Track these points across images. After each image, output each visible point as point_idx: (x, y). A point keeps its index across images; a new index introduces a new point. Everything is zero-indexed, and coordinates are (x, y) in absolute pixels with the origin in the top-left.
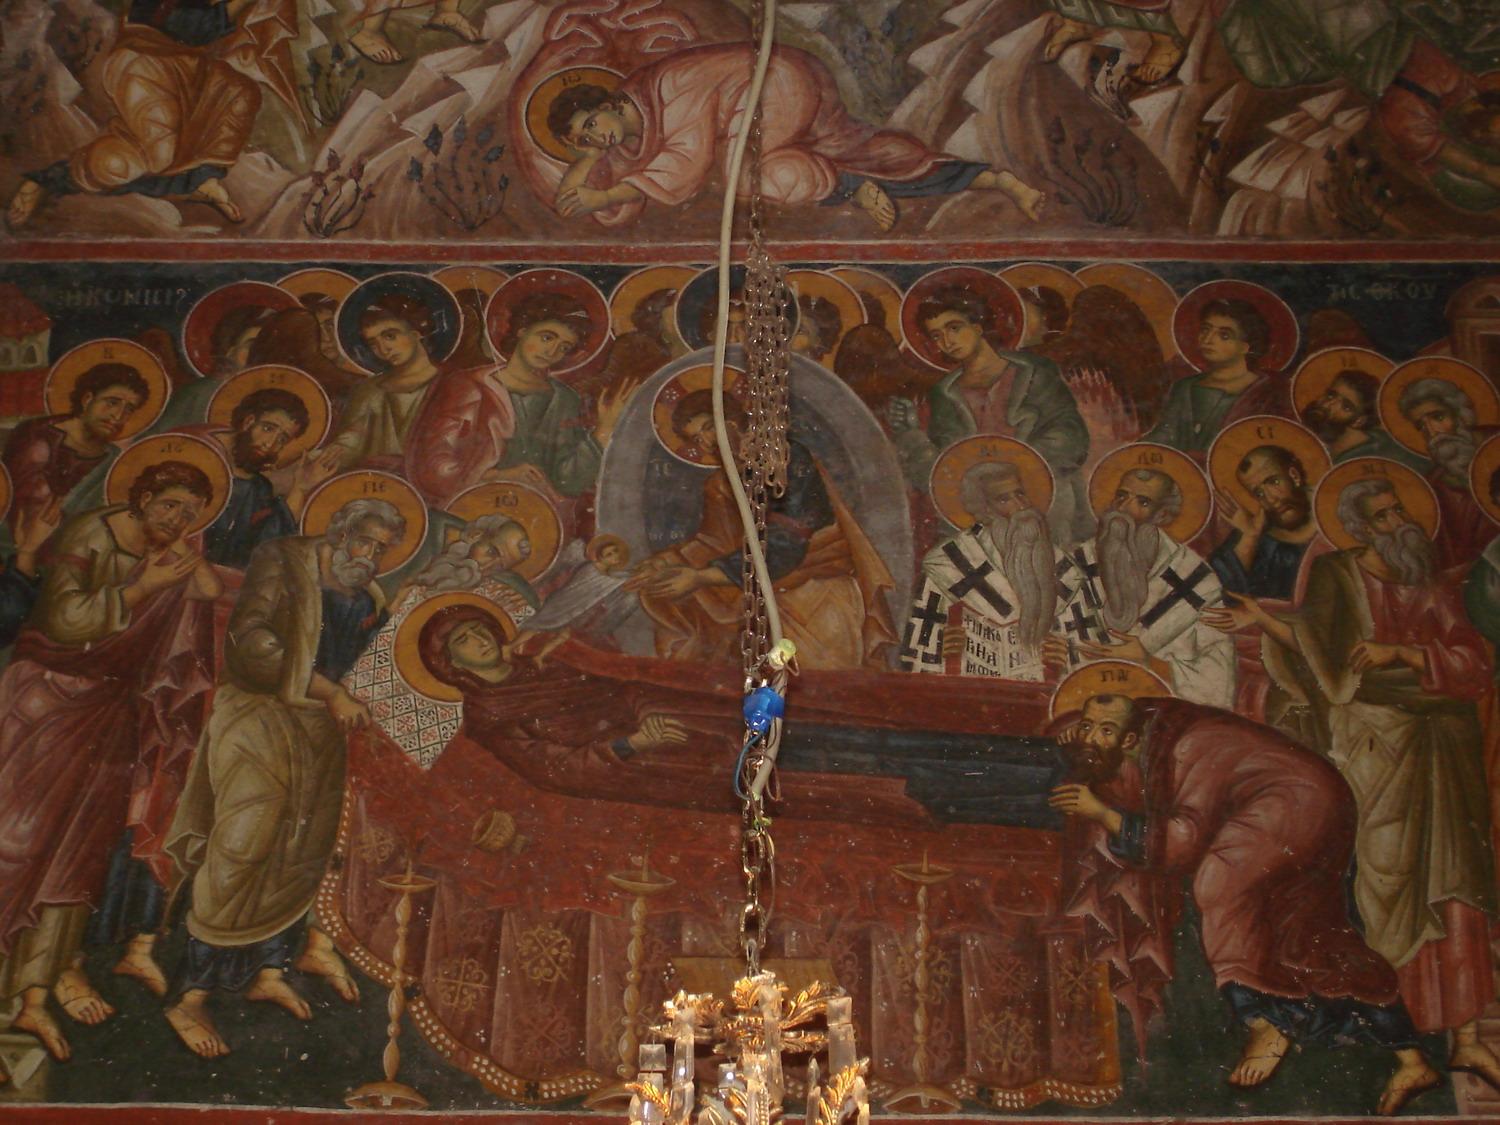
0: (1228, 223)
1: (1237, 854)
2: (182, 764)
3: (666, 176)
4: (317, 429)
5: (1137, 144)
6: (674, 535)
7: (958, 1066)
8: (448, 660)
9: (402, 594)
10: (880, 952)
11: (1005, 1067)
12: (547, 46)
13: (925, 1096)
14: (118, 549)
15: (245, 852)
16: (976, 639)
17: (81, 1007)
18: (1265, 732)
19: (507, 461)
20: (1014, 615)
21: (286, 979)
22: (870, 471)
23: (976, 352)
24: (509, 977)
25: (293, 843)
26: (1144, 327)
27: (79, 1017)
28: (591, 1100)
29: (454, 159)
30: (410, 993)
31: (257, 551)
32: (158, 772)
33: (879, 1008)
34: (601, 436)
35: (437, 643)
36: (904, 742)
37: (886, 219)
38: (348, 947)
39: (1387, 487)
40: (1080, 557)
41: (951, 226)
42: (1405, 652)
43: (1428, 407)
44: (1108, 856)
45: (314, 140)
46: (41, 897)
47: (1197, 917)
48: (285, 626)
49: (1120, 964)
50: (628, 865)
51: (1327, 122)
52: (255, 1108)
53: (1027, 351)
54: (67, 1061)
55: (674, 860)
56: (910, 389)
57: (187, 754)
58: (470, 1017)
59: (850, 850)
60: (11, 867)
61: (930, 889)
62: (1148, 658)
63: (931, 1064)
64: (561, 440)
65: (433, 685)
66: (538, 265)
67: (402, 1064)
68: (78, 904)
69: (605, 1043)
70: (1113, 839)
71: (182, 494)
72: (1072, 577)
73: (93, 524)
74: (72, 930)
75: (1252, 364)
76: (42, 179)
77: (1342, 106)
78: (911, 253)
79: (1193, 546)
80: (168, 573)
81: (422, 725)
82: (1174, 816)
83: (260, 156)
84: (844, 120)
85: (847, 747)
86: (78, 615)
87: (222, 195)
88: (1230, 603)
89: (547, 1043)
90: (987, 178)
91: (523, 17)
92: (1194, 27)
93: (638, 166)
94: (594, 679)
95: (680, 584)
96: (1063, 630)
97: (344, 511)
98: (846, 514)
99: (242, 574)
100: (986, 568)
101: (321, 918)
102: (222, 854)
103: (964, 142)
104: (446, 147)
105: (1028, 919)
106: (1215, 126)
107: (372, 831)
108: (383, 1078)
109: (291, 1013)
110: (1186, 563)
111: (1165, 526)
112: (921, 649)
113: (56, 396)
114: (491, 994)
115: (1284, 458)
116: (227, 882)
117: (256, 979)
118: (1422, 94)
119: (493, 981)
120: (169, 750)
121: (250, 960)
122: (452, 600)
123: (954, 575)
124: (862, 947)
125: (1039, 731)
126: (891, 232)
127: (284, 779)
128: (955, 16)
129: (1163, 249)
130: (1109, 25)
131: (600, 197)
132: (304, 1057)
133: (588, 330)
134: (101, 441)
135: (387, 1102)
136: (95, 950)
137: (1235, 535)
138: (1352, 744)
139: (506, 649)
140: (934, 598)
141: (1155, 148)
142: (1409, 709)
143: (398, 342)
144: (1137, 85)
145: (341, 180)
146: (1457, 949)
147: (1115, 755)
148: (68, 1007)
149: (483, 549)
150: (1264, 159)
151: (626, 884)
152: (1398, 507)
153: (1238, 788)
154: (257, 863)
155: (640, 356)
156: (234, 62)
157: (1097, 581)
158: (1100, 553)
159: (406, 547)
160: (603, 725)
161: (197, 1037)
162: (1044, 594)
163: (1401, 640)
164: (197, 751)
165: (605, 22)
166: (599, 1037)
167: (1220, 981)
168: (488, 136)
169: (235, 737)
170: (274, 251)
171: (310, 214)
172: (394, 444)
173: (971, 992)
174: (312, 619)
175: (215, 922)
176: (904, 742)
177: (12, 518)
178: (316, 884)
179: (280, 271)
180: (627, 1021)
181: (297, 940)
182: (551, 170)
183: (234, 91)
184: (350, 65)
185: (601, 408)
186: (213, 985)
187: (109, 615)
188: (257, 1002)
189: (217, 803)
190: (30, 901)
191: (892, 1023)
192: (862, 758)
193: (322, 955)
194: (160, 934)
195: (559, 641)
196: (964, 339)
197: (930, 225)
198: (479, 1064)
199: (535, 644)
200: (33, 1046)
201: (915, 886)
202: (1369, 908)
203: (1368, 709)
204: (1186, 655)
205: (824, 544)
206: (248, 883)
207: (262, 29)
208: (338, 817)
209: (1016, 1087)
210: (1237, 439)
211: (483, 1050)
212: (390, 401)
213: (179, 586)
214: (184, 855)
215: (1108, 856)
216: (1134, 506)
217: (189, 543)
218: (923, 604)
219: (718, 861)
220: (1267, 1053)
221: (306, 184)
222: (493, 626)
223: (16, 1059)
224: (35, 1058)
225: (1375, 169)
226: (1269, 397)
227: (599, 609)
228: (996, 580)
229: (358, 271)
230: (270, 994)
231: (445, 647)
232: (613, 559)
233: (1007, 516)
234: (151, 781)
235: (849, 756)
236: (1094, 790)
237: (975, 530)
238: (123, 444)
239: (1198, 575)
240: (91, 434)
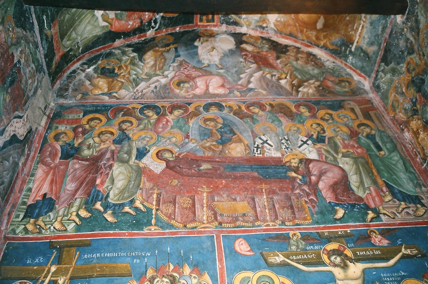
0: (300, 95)
1: (326, 181)
2: (108, 174)
3: (198, 91)
4: (134, 125)
5: (281, 86)
6: (205, 138)
7: (277, 218)
8: (162, 157)
9: (152, 147)
10: (257, 200)
11: (287, 218)
12: (175, 76)
13: (271, 224)
14: (95, 143)
16: (267, 151)
18: (326, 162)
19: (172, 127)
20: (273, 147)
21: (130, 208)
22: (242, 128)
23: (259, 112)
24: (178, 207)
25: (131, 186)
26: (289, 108)
28: (198, 228)
29: (159, 90)
30: (157, 210)
31: (123, 142)
33: (258, 209)
34: (190, 124)
35: (159, 154)
36: (256, 167)
37: (239, 95)
38: (143, 202)
39: (338, 127)
40: (284, 138)
41: (251, 96)
42: (349, 150)
43: (342, 117)
44: (300, 183)
45: (133, 88)
47: (321, 191)
48: (129, 153)
49: (307, 200)
50: (202, 187)
51: (314, 83)
52: (123, 232)
53: (268, 111)
54: (80, 225)
55: (212, 186)
56: (248, 117)
57: (109, 173)
58: (170, 214)
59: (248, 183)
61: (265, 190)
62: (301, 152)
63: (271, 218)
64: (182, 125)
65: (159, 161)
66: (176, 102)
67: (156, 223)
69: (200, 217)
70: (300, 180)
71: (109, 135)
72: (283, 141)
73: (91, 139)
75: (309, 112)
76: (83, 94)
77: (316, 81)
78: (244, 99)
79: (305, 136)
80: (106, 146)
81: (158, 167)
82: (312, 176)
83: (124, 90)
84: (229, 83)
85: (245, 168)
86: (86, 153)
87: (116, 95)
88: (314, 144)
89: (188, 218)
90: (256, 90)
91: (171, 72)
92: (288, 72)
93: (193, 90)
94: (192, 159)
95: (208, 144)
96: (284, 149)
97: (140, 136)
98: (238, 134)
99: (120, 146)
100: (267, 140)
103: (251, 86)
104: (158, 89)
105: (286, 194)
106: (294, 84)
107: (148, 184)
108: (152, 225)
109: (132, 214)
110: (305, 139)
111: (300, 134)
112: (257, 153)
113: (84, 121)
114: (175, 210)
115: (319, 125)
117: (123, 208)
118: (329, 80)
119: (175, 207)
120: (104, 173)
121: (122, 205)
122: (163, 148)
123: (262, 142)
124: (253, 199)
125: (282, 164)
126: (241, 97)
128: (246, 71)
129: (290, 98)
130: (273, 72)
131: (186, 94)
132: (134, 222)
133: (186, 110)
134: (92, 128)
135: (153, 229)
136: (88, 204)
137: (312, 135)
138: (343, 164)
139: (174, 155)
140: (258, 145)
141: (285, 86)
142: (353, 158)
143: (150, 113)
144: (280, 79)
145: (139, 93)
146: (374, 194)
147: (298, 167)
149: (168, 141)
150: (304, 88)
151: (202, 190)
152: (341, 130)
153: (323, 171)
154: (123, 189)
155: (196, 114)
156: (119, 79)
157: (288, 142)
158: (288, 137)
159: (153, 141)
160: (194, 166)
161: (110, 219)
162: (279, 144)
163: (347, 148)
164: (111, 172)
165: (185, 73)
166: (199, 216)
167: (328, 201)
168: (165, 87)
169: (119, 170)
170: (127, 102)
171: (133, 97)
172: (150, 127)
173: (277, 206)
174: (134, 152)
176: (256, 167)
177: (74, 139)
178: (136, 192)
179: (127, 104)
180: (204, 213)
181: (132, 202)
182: (177, 91)
183: (119, 83)
184: (140, 79)
185: (189, 120)
186: (114, 209)
187: (93, 152)
191: (262, 211)
192: (248, 169)
193: (138, 204)
195: (184, 154)
196: (257, 110)
197: (247, 96)
198: (173, 222)
199: (179, 154)
201: (262, 189)
202: (355, 189)
203: (345, 159)
204: (308, 152)
205: (235, 138)
207: (124, 76)
208: (141, 181)
209: (290, 221)
210: (311, 121)
211: (174, 219)
212: (149, 121)
213: (107, 148)
215: (300, 183)
216: (293, 131)
217: (109, 142)
218: (256, 146)
219: (221, 186)
220: (340, 213)
221: (133, 93)
222: (171, 152)
225: (323, 89)
226: (314, 116)
227: (192, 149)
228: (269, 142)
229: (142, 104)
231: (161, 155)
232: (194, 141)
233: (269, 133)
235: (245, 169)
236: (295, 172)
237: (264, 135)
238: (97, 128)
239: (307, 141)
240: (90, 127)
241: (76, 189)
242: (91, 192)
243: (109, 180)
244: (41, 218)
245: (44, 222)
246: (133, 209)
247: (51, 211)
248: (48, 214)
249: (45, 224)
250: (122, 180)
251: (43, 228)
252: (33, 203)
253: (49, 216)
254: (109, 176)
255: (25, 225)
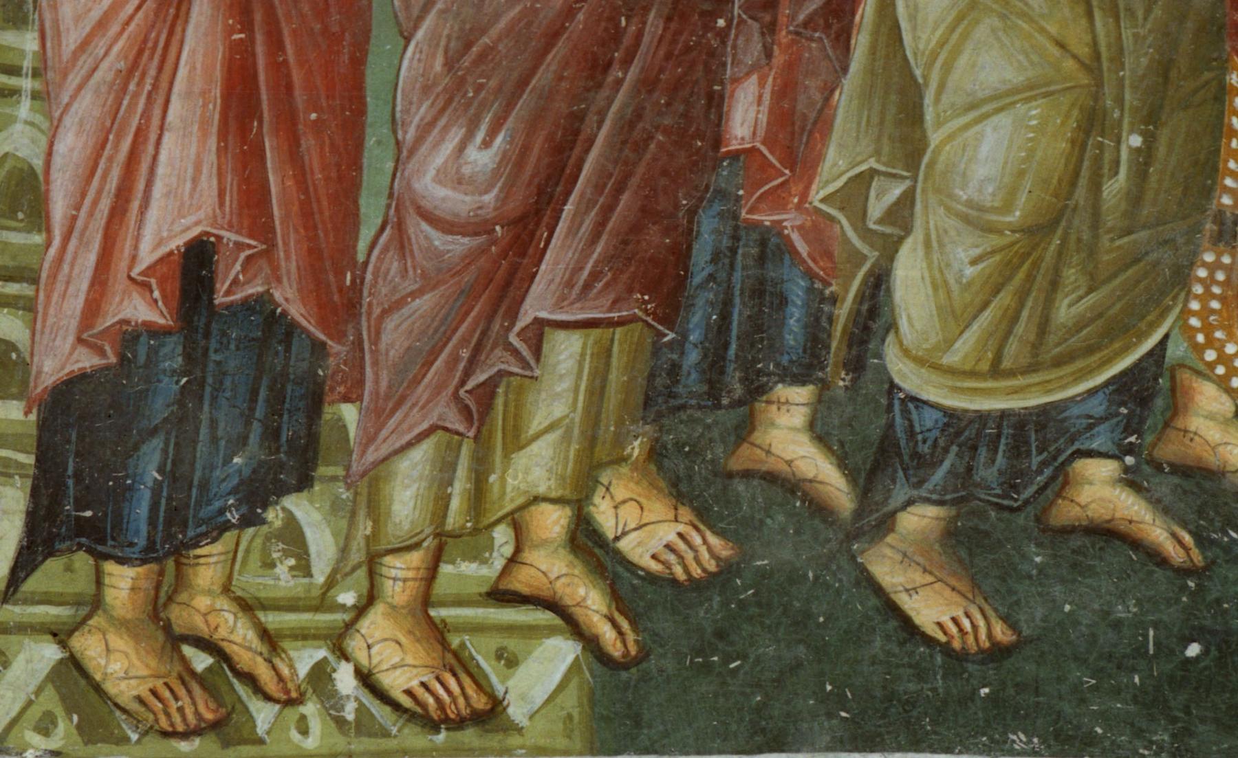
15: (1007, 207)
17: (656, 545)
21: (1131, 480)
25: (1115, 187)
27: (655, 566)
32: (783, 36)
46: (536, 306)
60: (460, 245)
68: (621, 323)
74: (616, 377)
101: (1199, 349)
102: (948, 209)
116: (969, 271)
121: (1041, 443)
127: (1084, 51)
132: (1193, 650)
136: (682, 418)
148: (624, 545)
161: (934, 608)
175: (952, 358)
178: (1181, 278)
186: (960, 494)
188: (1068, 531)
189: (928, 99)
190: (513, 315)
194: (824, 385)
200: (551, 631)
206: (1021, 275)
214: (862, 215)
223: (512, 662)
224: (556, 657)
230: (1098, 512)
234: (769, 55)
241: (515, 206)
242: (682, 254)
243: (866, 94)
244: (208, 566)
245: (247, 606)
246: (1164, 486)
247: (304, 483)
248: (274, 516)
249: (265, 634)
250: (1003, 100)
251: (250, 679)
252: (86, 361)
253: (293, 537)
254: (861, 43)
255: (60, 634)
